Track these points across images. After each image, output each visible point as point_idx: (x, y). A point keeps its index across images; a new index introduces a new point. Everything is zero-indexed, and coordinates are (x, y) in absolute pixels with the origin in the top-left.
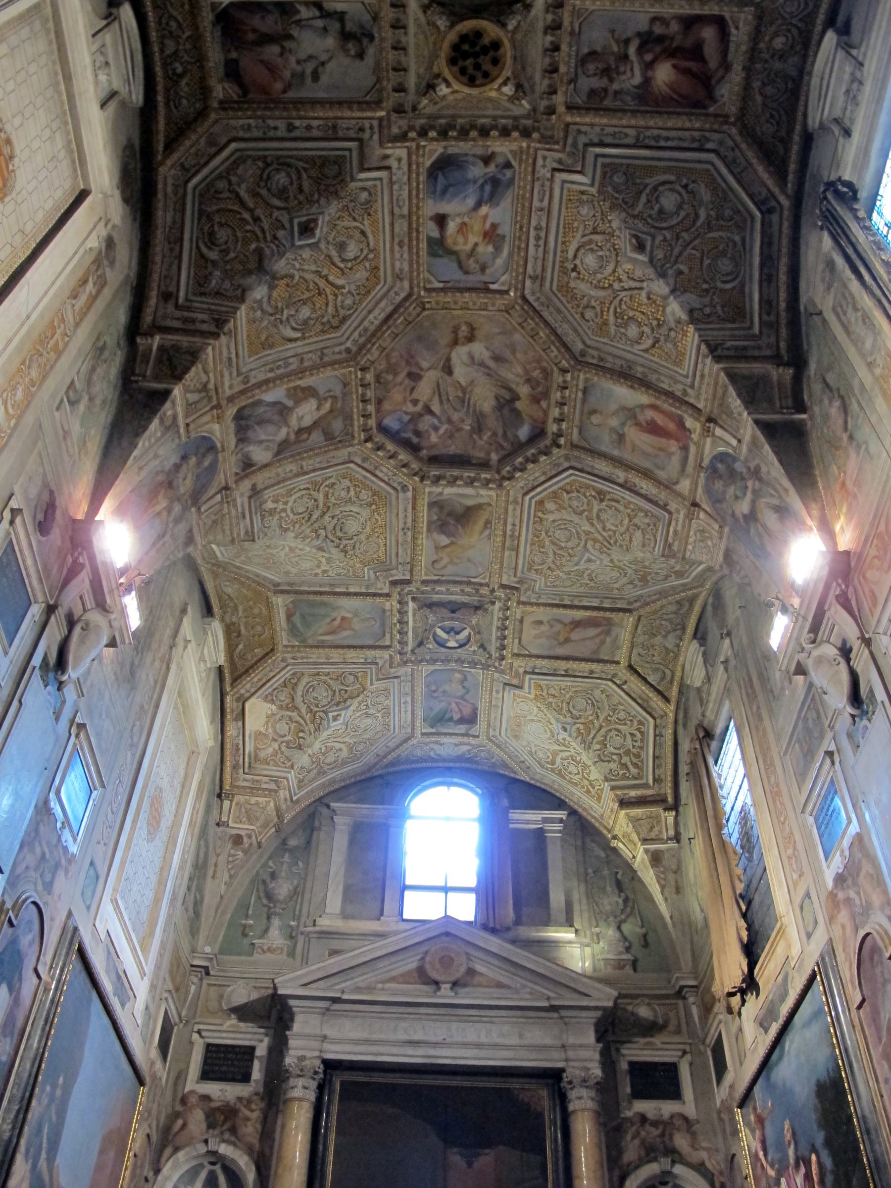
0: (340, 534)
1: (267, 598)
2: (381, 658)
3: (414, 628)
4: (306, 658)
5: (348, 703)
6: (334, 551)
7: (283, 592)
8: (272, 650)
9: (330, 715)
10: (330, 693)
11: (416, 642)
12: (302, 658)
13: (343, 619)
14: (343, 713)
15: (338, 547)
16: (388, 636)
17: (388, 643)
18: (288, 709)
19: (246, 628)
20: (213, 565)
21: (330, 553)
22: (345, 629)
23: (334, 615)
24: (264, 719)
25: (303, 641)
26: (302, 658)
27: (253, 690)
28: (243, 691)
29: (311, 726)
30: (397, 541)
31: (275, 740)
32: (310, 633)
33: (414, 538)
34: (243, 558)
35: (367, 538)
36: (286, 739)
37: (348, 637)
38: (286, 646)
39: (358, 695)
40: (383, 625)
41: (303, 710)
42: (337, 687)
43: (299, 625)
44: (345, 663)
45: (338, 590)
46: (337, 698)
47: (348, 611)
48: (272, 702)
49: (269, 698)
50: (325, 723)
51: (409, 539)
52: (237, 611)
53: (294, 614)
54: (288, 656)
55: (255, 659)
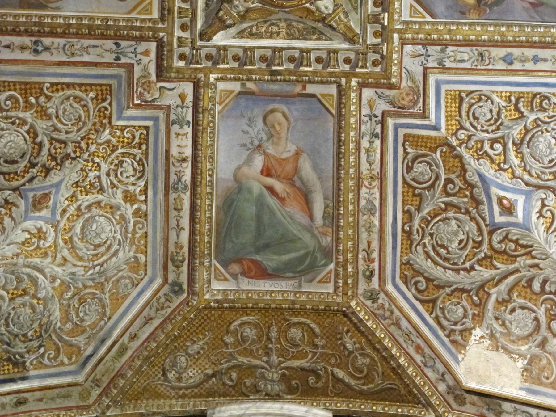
0: (22, 166)
1: (208, 308)
2: (371, 105)
3: (290, 36)
4: (368, 251)
5: (475, 179)
6: (55, 177)
7: (191, 279)
8: (345, 315)
9: (499, 219)
10: (451, 214)
11: (329, 32)
12: (369, 260)
13: (267, 172)
14: (495, 191)
15: (47, 171)
16: (311, 89)
17: (333, 90)
18: (481, 305)
19: (294, 358)
20: (105, 392)
21: (58, 185)
22: (296, 170)
23: (256, 188)
24: (501, 358)
25: (327, 254)
26: (369, 260)
27: (442, 368)
28: (442, 387)
29: (522, 261)
30: (60, 64)
31: (543, 344)
32: (307, 238)
33: (52, 34)
34: (80, 340)
35: (49, 118)
36: (543, 319)
37: (315, 167)
38: (336, 288)
39: (460, 157)
40: (286, 97)
41: (486, 273)
42: (441, 200)
43: (286, 257)
44: (382, 177)
45: (187, 178)
46: (463, 201)
47: (249, 161)
48: (466, 332)
49: (458, 338)
50: (515, 233)
51: (62, 41)
52: (251, 368)
53: (254, 262)
54: (362, 285)
55: (369, 351)
